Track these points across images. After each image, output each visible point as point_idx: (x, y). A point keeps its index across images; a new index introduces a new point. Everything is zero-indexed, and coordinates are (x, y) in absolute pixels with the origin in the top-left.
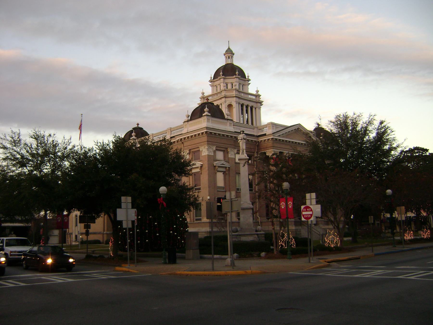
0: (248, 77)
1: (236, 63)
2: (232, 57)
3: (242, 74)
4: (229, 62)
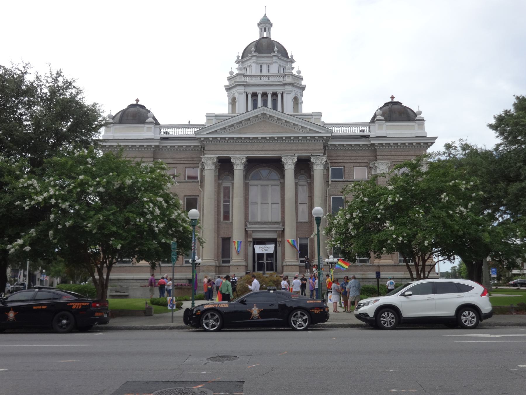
0: (292, 56)
1: (275, 35)
3: (283, 52)
4: (265, 36)
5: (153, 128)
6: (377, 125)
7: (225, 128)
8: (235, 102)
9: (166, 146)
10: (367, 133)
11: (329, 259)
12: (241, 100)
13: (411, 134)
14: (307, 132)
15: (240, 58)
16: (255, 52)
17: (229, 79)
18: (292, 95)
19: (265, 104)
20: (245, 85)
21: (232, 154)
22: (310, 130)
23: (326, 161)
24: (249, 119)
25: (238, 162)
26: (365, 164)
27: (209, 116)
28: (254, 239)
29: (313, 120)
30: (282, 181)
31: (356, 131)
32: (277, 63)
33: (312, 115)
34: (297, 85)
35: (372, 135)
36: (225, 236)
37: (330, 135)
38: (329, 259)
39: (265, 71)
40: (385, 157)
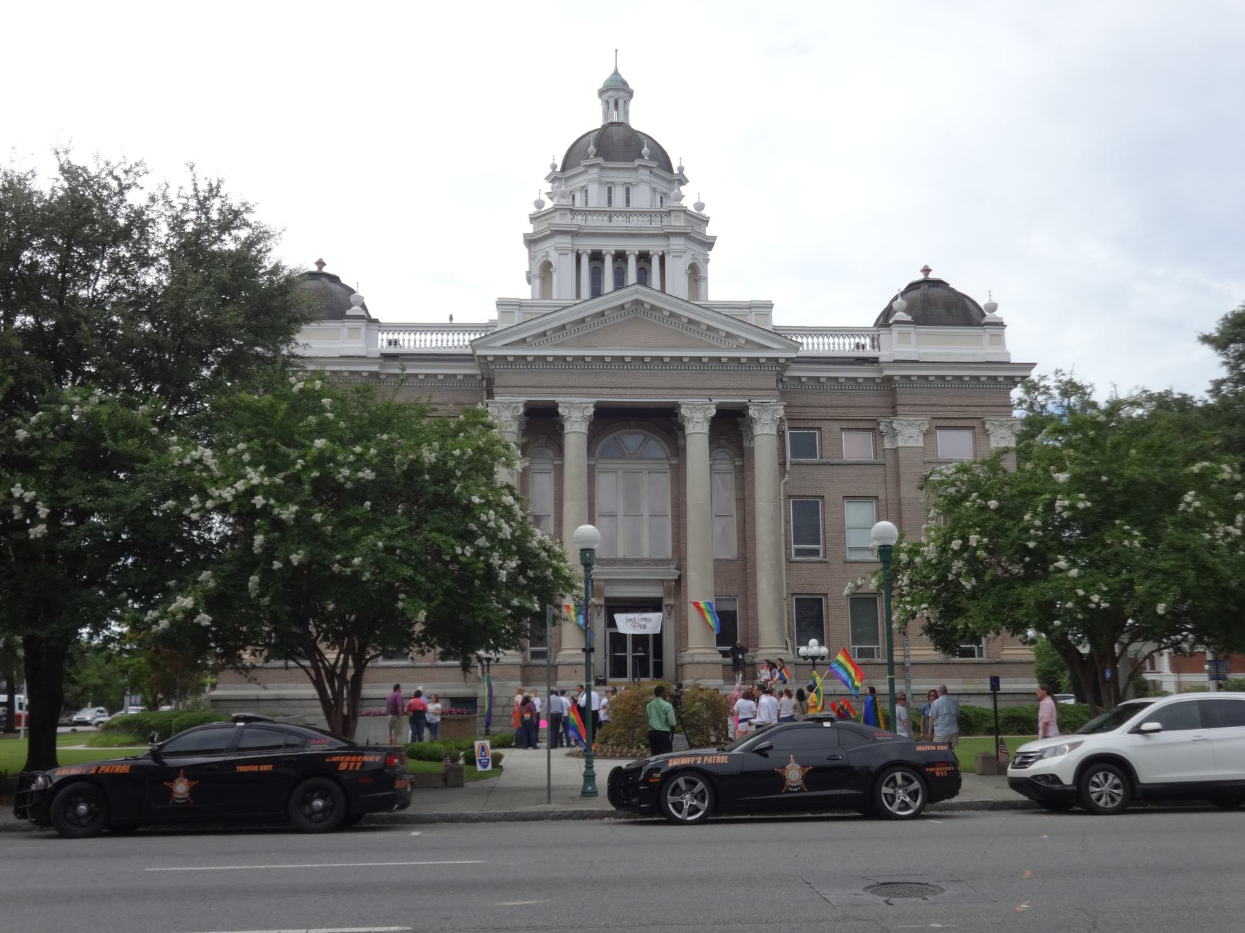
0: (681, 169)
1: (640, 119)
2: (626, 103)
3: (661, 159)
5: (363, 329)
6: (895, 334)
7: (544, 334)
8: (551, 274)
9: (416, 375)
10: (869, 352)
12: (564, 269)
13: (974, 355)
14: (739, 348)
15: (558, 169)
16: (596, 155)
17: (533, 219)
18: (686, 260)
19: (643, 277)
20: (574, 234)
21: (559, 395)
22: (747, 341)
24: (602, 314)
25: (576, 415)
26: (869, 425)
27: (503, 305)
28: (607, 600)
29: (752, 319)
30: (674, 462)
31: (847, 347)
32: (648, 183)
33: (750, 306)
34: (695, 234)
35: (885, 355)
39: (619, 203)
40: (917, 408)
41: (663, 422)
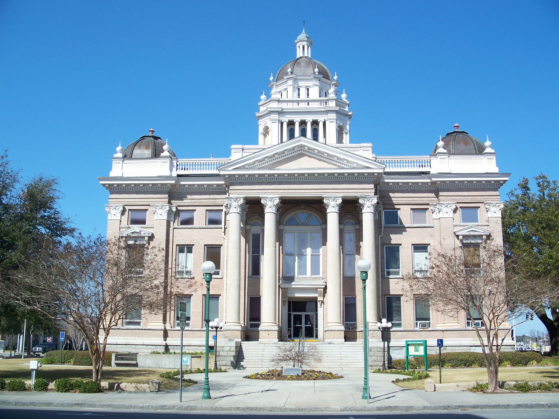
11: (381, 323)
19: (303, 133)
23: (378, 203)
30: (323, 227)
36: (254, 295)
37: (382, 171)
38: (381, 323)
39: (303, 96)
41: (317, 206)
